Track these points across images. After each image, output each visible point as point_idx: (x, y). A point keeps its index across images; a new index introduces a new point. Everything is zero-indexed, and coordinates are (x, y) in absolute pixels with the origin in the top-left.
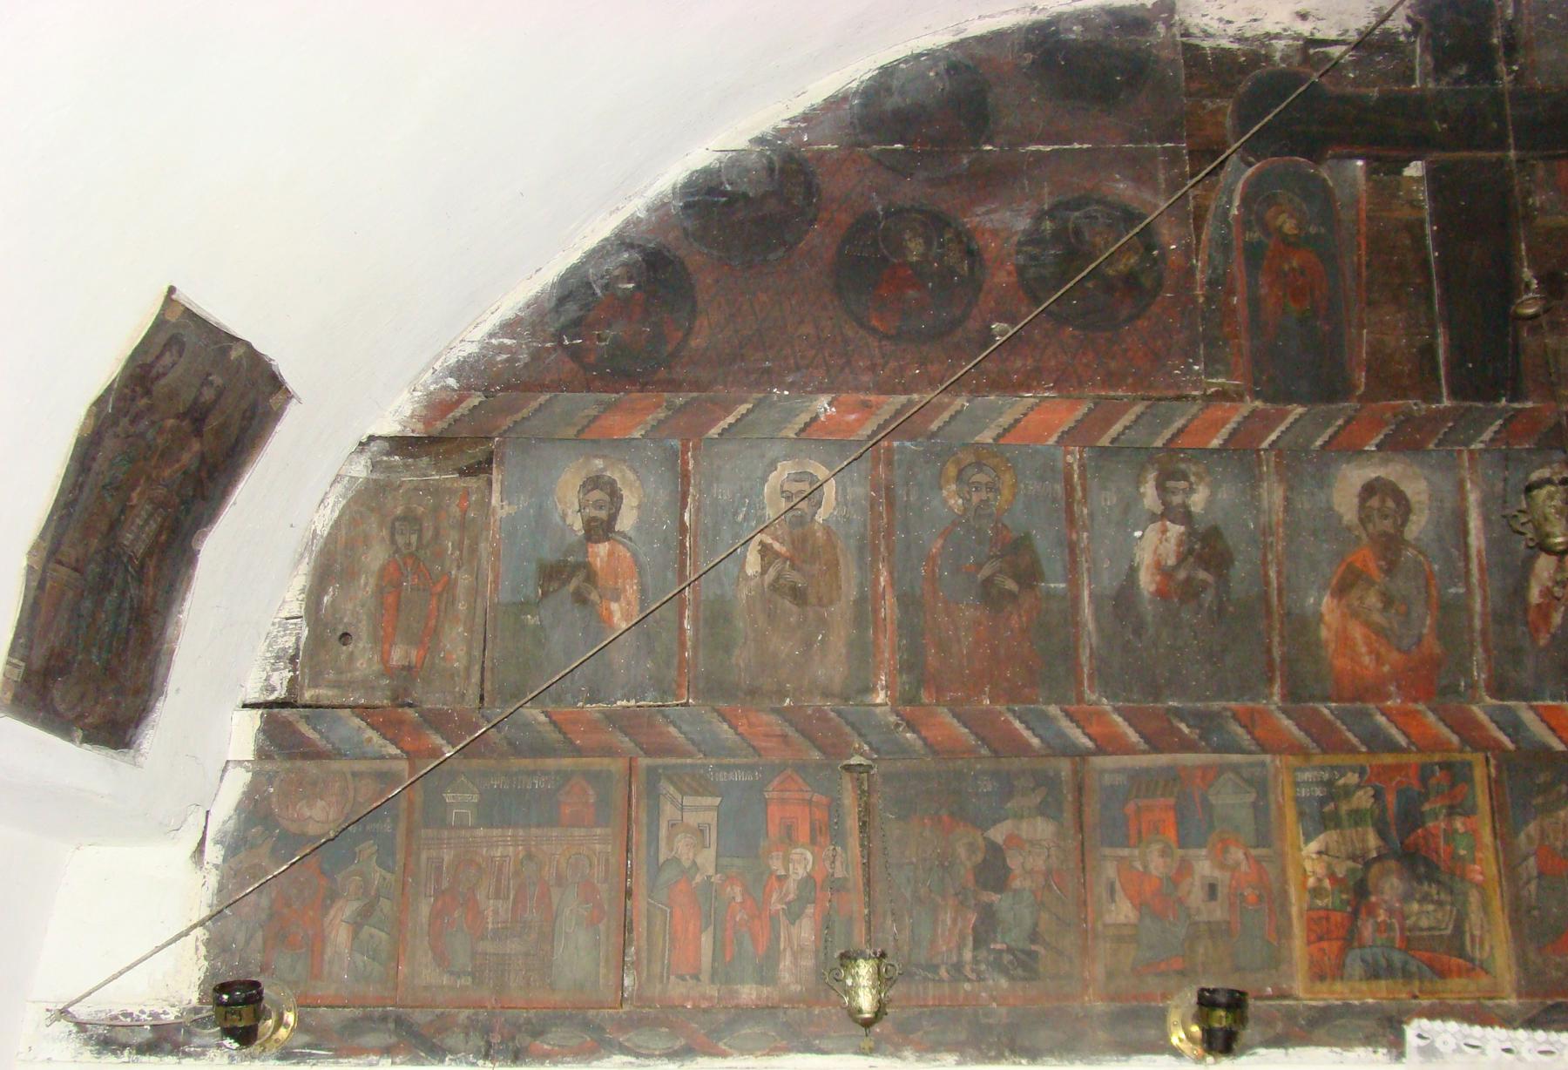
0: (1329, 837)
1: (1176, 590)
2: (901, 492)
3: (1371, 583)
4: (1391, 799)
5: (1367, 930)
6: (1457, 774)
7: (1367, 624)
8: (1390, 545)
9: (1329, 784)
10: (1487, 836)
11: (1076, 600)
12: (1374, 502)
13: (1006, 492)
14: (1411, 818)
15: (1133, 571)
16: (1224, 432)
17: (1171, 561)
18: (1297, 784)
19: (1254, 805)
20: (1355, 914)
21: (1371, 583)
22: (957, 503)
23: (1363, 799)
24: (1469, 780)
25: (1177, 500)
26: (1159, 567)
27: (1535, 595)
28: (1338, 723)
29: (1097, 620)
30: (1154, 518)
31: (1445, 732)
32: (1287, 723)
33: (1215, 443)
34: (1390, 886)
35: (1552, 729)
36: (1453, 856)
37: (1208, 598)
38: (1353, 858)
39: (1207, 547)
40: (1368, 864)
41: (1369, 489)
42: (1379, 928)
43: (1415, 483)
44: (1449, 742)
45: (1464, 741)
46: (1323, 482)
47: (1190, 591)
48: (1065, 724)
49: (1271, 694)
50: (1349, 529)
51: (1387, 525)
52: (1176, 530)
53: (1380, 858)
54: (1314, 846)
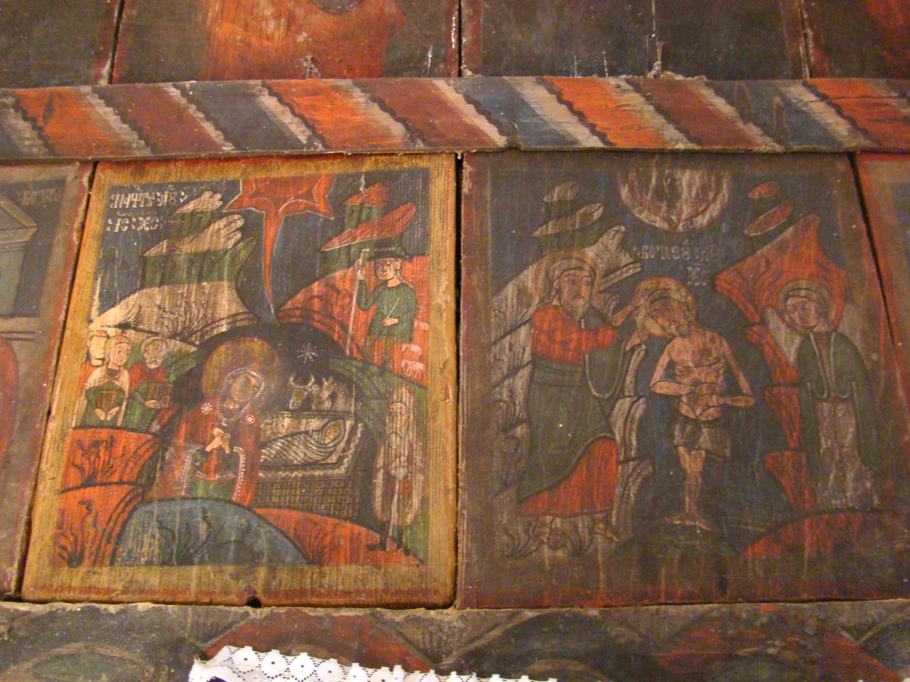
0: (148, 301)
4: (272, 233)
5: (183, 469)
6: (402, 191)
9: (171, 209)
10: (442, 293)
14: (306, 261)
18: (110, 214)
19: (27, 248)
20: (164, 439)
23: (223, 235)
24: (422, 200)
28: (192, 109)
31: (384, 119)
34: (244, 384)
35: (581, 116)
36: (373, 328)
38: (184, 335)
40: (209, 346)
42: (202, 462)
44: (387, 135)
45: (413, 132)
49: (98, 76)
53: (235, 334)
54: (116, 314)
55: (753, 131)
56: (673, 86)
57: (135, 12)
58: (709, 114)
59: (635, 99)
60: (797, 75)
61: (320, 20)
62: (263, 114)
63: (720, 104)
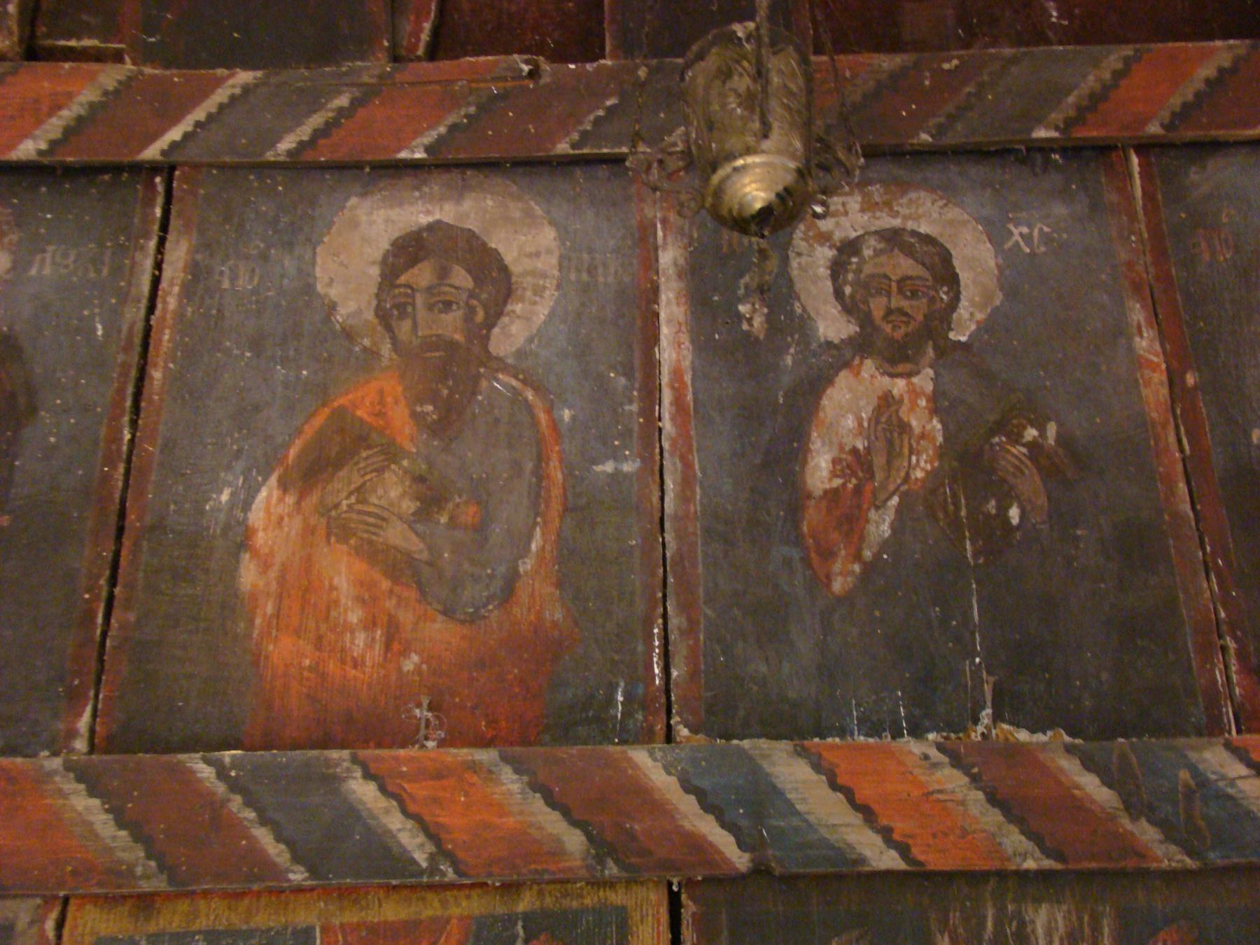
3: (391, 453)
7: (372, 553)
8: (452, 375)
12: (422, 275)
16: (54, 126)
21: (391, 453)
27: (820, 470)
28: (236, 801)
31: (552, 823)
32: (84, 804)
33: (27, 150)
35: (867, 813)
41: (410, 249)
43: (529, 236)
44: (557, 851)
45: (601, 846)
46: (300, 232)
49: (72, 734)
50: (349, 334)
51: (450, 325)
55: (1147, 833)
56: (1014, 751)
57: (132, 617)
58: (1077, 807)
59: (952, 780)
60: (1213, 728)
61: (441, 633)
62: (352, 813)
63: (1091, 785)
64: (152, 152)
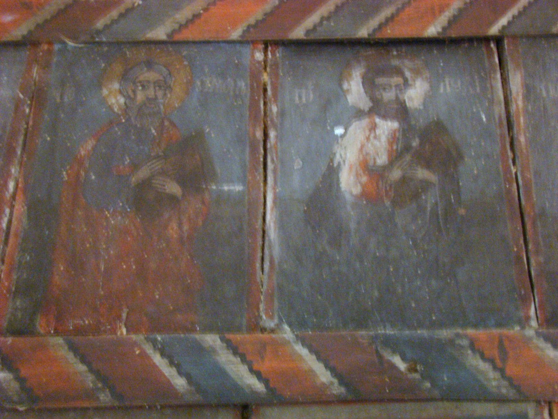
1: (387, 190)
2: (56, 94)
11: (254, 206)
13: (178, 90)
15: (332, 172)
17: (382, 160)
22: (117, 102)
25: (388, 96)
26: (366, 167)
29: (281, 225)
30: (359, 114)
37: (430, 199)
39: (429, 143)
47: (407, 192)
48: (227, 360)
52: (387, 127)
57: (541, 259)
64: (494, 30)
